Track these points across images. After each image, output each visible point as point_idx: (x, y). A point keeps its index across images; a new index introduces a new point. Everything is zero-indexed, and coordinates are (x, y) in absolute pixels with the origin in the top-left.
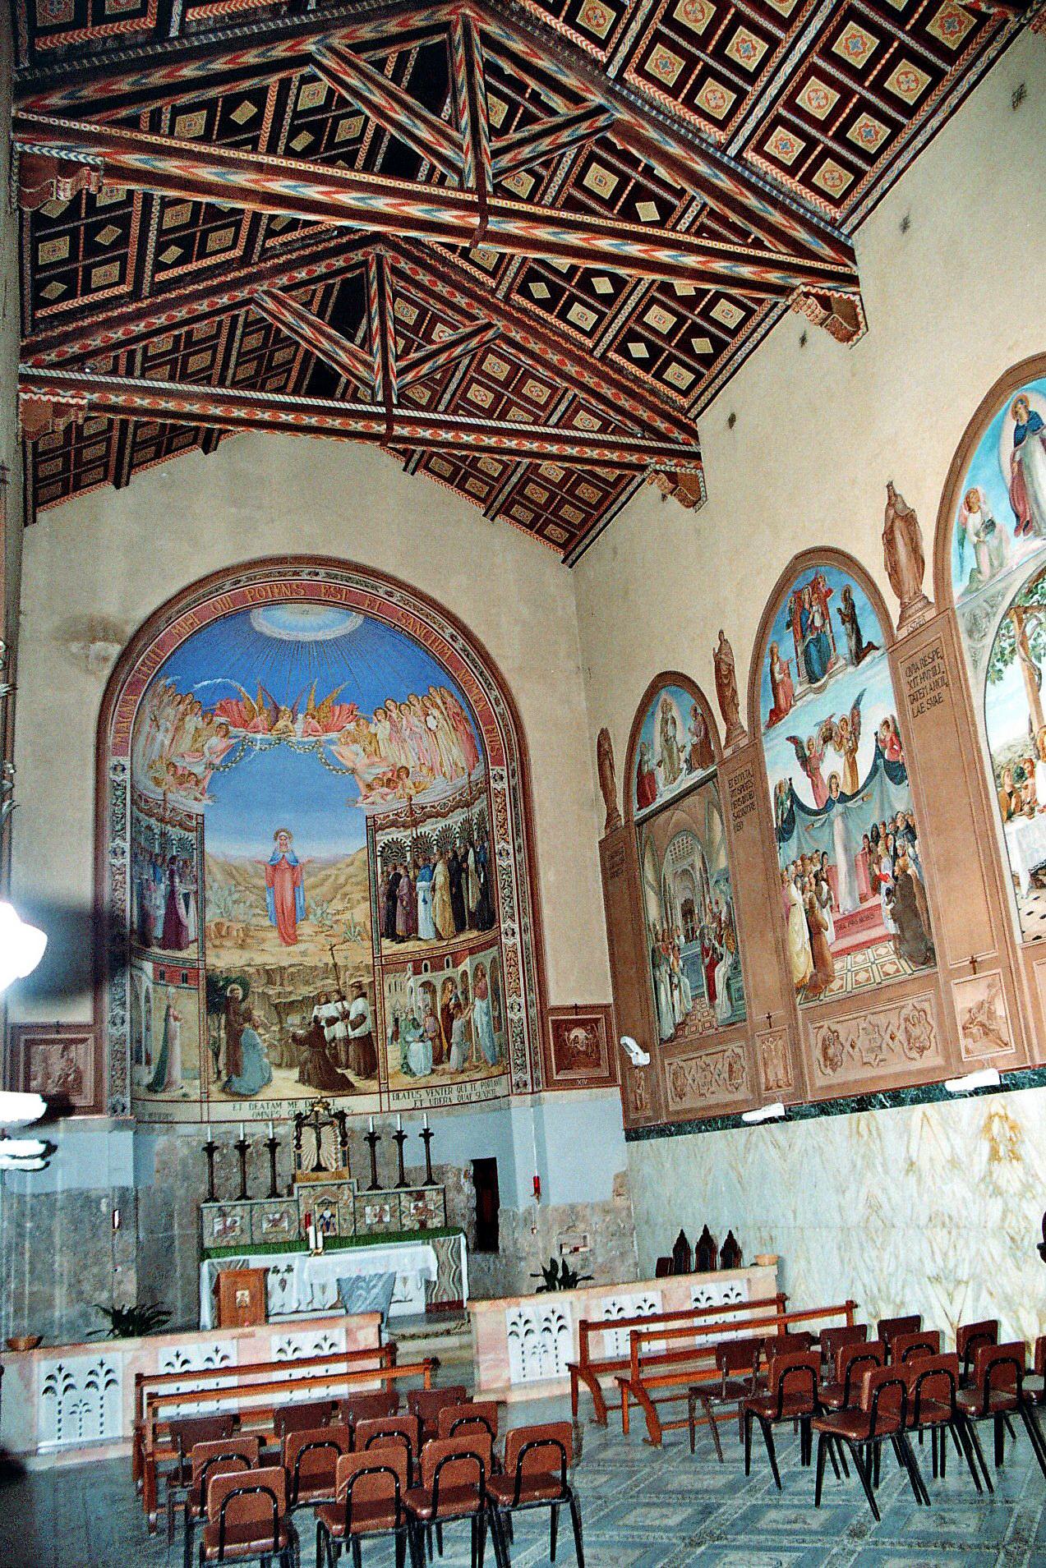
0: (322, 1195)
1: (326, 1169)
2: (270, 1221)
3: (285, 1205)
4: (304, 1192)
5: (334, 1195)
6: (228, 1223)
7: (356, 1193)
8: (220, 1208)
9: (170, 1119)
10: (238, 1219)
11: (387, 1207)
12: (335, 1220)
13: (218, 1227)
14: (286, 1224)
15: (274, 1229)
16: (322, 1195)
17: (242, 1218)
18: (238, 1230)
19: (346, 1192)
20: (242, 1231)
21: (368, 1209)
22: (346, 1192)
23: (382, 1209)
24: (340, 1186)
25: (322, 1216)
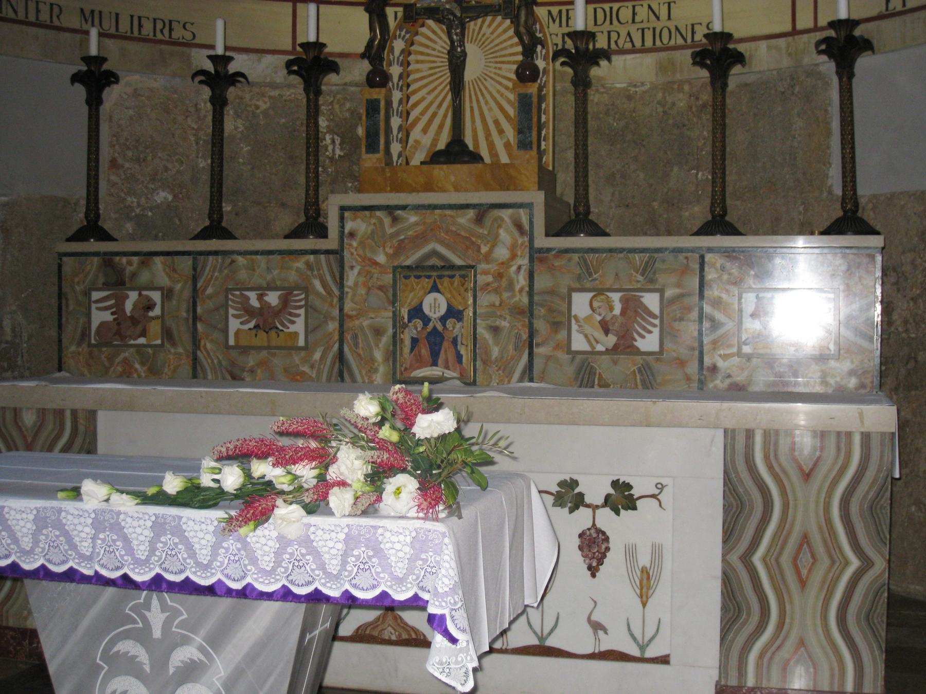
0: (420, 239)
1: (475, 158)
2: (250, 312)
3: (300, 264)
4: (357, 225)
5: (468, 244)
6: (129, 306)
7: (542, 241)
8: (108, 260)
9: (178, 33)
10: (156, 296)
11: (651, 301)
12: (455, 328)
13: (100, 317)
14: (298, 326)
15: (261, 339)
16: (420, 239)
17: (168, 294)
18: (155, 328)
19: (506, 236)
20: (167, 334)
21: (581, 303)
22: (506, 236)
23: (632, 306)
24: (482, 212)
25: (417, 312)
